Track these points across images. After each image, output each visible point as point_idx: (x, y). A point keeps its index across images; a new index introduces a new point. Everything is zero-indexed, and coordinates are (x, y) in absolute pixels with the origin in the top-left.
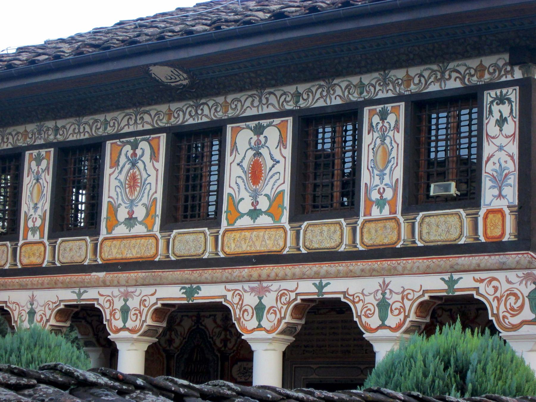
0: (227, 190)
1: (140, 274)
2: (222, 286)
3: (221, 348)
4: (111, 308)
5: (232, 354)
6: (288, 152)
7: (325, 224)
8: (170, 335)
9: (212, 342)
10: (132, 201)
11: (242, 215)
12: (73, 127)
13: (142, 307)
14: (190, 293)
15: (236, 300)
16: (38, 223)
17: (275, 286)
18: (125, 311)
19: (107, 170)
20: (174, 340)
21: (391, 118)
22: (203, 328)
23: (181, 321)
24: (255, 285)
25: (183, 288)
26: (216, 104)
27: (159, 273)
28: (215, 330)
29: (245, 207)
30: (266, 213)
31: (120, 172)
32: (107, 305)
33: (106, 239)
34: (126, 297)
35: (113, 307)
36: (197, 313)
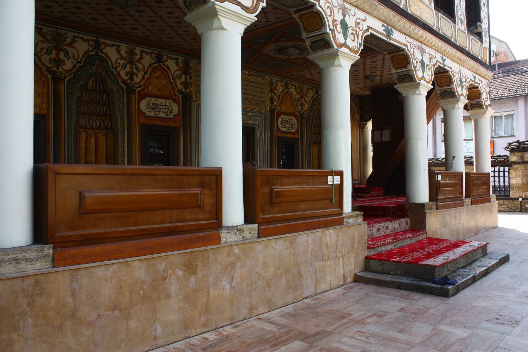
2: (404, 36)
3: (127, 80)
4: (332, 16)
5: (139, 89)
7: (446, 20)
8: (58, 54)
9: (115, 73)
13: (358, 30)
17: (428, 50)
18: (345, 26)
20: (64, 61)
22: (104, 56)
23: (74, 41)
24: (419, 44)
25: (383, 26)
28: (119, 61)
35: (334, 16)
36: (96, 38)
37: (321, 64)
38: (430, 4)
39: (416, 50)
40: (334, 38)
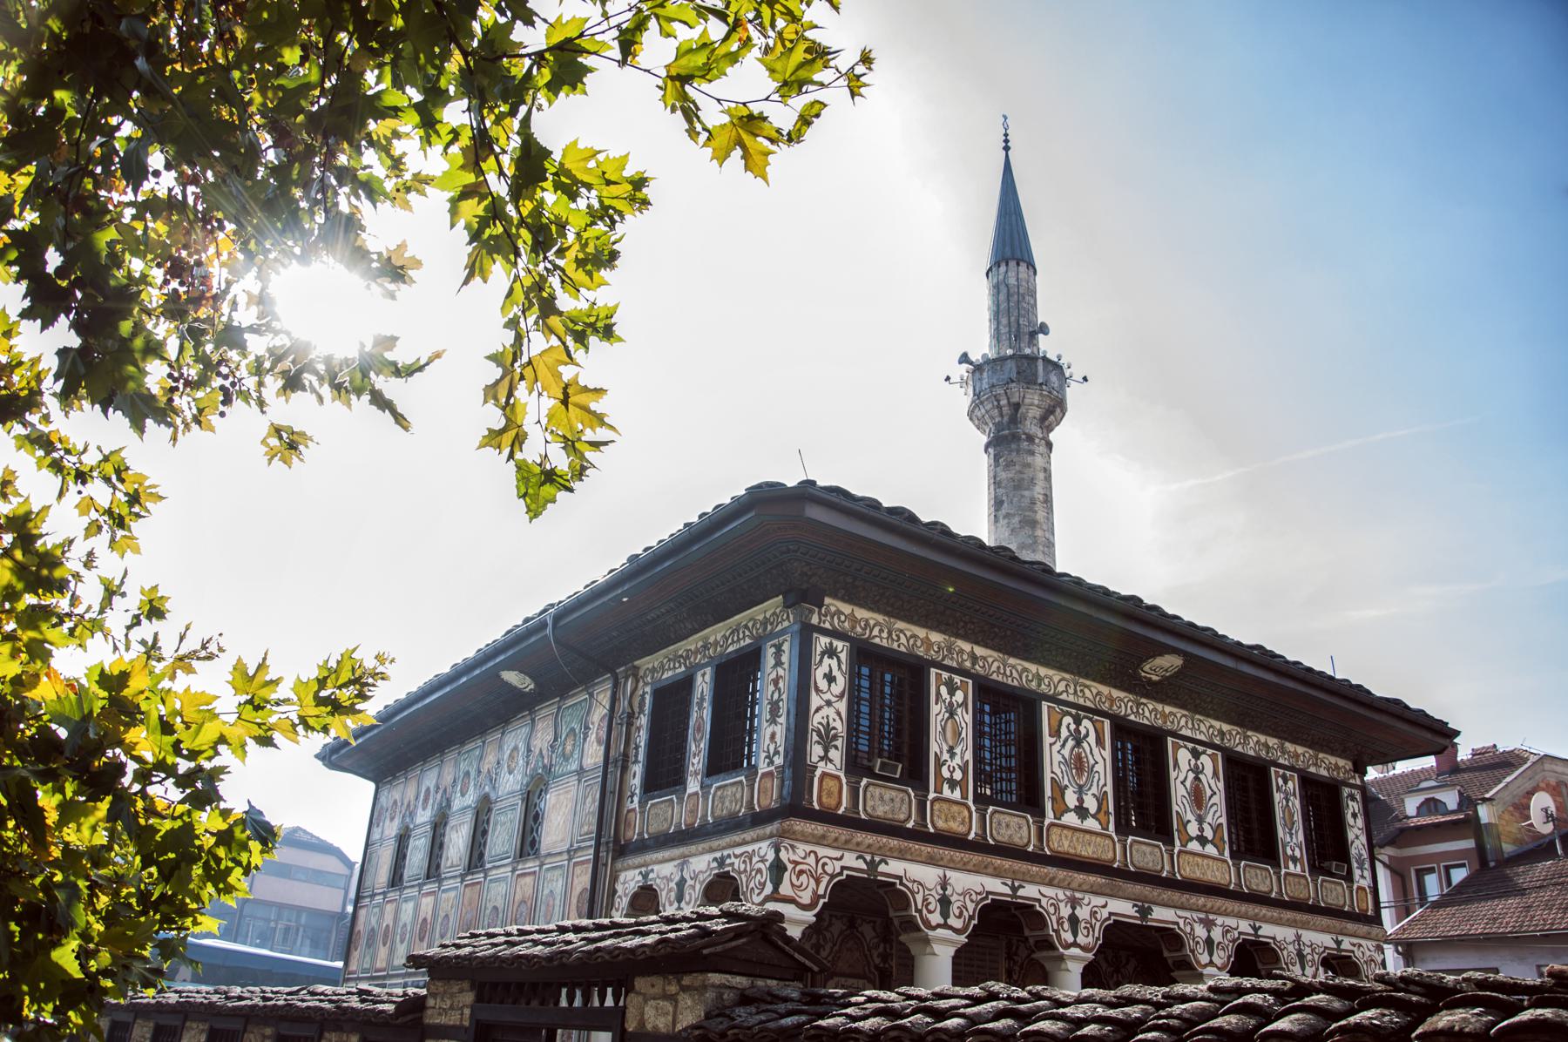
0: (1175, 808)
1: (1100, 880)
2: (1172, 911)
6: (1221, 785)
10: (1080, 787)
11: (1191, 839)
12: (996, 664)
14: (1144, 912)
15: (1188, 929)
16: (958, 775)
17: (1220, 920)
18: (1074, 921)
19: (1047, 740)
21: (1290, 784)
24: (1202, 916)
26: (1155, 709)
27: (1120, 882)
29: (1193, 829)
30: (1212, 842)
31: (1063, 746)
32: (1052, 910)
33: (1052, 825)
34: (1074, 903)
37: (1048, 966)
38: (1221, 853)
39: (1196, 926)
40: (1059, 936)
